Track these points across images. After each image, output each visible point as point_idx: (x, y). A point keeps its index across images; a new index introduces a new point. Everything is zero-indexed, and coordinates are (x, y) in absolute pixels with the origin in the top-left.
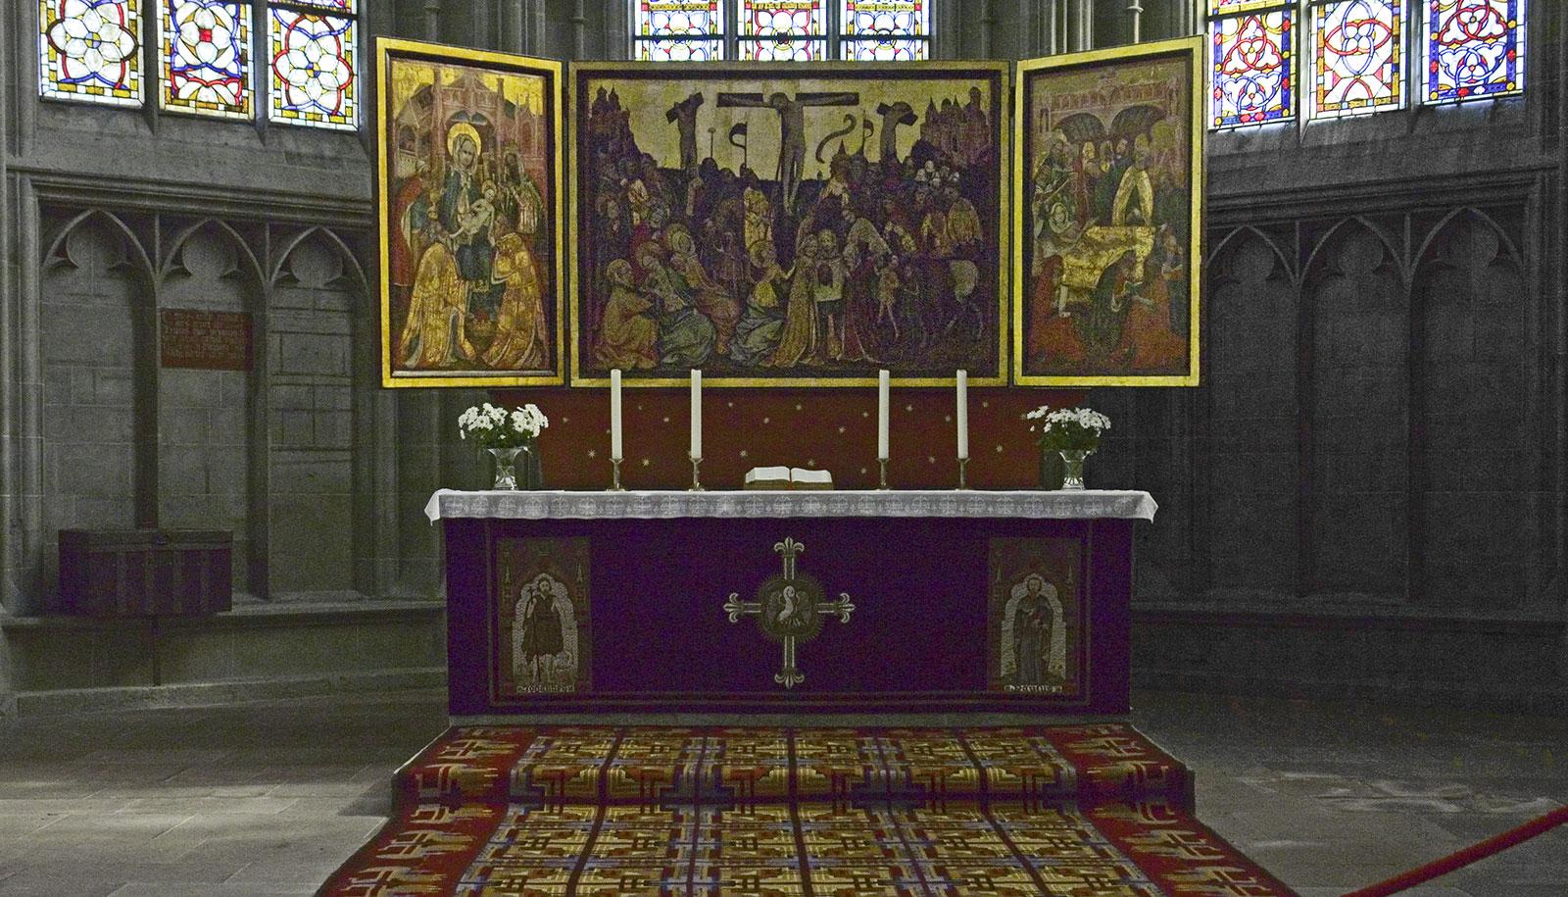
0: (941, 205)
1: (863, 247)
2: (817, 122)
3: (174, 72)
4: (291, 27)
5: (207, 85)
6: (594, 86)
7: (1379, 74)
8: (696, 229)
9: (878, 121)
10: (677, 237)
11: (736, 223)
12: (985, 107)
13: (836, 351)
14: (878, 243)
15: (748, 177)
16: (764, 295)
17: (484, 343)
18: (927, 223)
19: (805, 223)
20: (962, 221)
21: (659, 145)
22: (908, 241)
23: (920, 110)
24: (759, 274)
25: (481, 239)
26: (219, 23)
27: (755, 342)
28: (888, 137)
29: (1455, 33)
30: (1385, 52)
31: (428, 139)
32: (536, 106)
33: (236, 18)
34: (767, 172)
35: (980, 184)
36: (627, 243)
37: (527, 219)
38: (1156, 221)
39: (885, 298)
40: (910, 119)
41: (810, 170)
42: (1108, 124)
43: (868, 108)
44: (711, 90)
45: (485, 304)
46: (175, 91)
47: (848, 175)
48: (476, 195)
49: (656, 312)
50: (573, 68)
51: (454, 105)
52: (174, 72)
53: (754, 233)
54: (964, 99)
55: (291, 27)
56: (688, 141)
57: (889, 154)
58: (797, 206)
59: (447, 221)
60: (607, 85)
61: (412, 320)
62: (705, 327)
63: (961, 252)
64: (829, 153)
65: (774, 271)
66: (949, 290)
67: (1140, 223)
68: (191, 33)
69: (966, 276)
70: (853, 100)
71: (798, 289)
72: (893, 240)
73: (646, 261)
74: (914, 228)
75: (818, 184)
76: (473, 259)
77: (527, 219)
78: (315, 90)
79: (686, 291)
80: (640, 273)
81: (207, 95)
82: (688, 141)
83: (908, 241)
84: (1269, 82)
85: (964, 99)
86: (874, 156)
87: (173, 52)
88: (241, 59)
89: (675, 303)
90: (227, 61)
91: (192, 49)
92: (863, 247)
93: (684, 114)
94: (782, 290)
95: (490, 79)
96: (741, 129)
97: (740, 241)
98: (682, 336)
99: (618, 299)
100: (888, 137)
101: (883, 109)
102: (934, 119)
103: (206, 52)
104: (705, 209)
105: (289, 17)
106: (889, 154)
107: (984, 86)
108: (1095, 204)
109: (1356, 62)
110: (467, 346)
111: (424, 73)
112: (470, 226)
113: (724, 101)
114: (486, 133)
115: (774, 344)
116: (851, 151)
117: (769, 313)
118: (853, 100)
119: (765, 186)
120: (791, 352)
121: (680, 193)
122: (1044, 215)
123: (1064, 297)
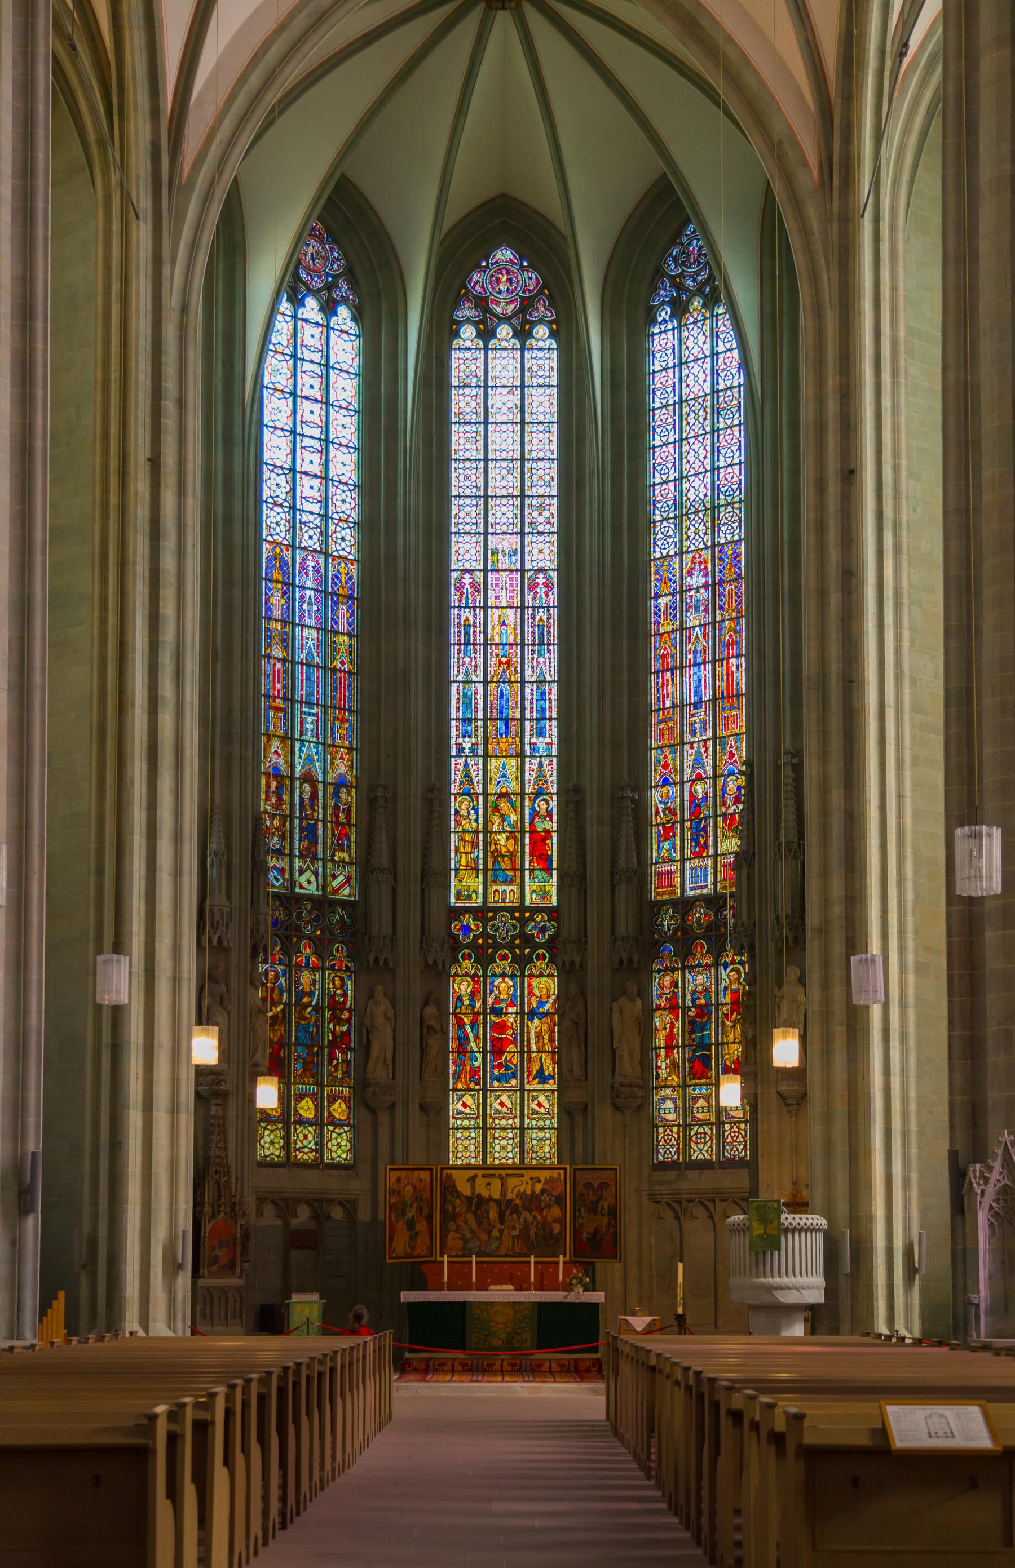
0: (549, 1207)
1: (526, 1220)
2: (512, 1182)
3: (296, 1150)
4: (333, 1131)
5: (306, 1153)
6: (445, 1172)
7: (707, 1151)
8: (476, 1215)
9: (530, 1182)
10: (470, 1216)
11: (487, 1212)
12: (562, 1178)
13: (517, 1249)
14: (530, 1218)
15: (491, 1199)
16: (495, 1233)
17: (413, 1248)
18: (544, 1213)
19: (508, 1212)
20: (555, 1212)
21: (465, 1189)
22: (539, 1217)
23: (543, 1180)
24: (494, 1227)
25: (413, 1218)
26: (310, 1132)
27: (493, 1247)
28: (533, 1186)
29: (729, 1139)
30: (709, 1144)
31: (399, 1192)
32: (428, 1179)
33: (315, 1130)
34: (497, 1196)
35: (560, 1200)
36: (454, 1217)
37: (426, 1212)
38: (609, 1215)
39: (532, 1234)
40: (539, 1181)
41: (510, 1196)
42: (596, 1186)
43: (526, 1178)
44: (480, 1173)
45: (414, 1236)
46: (296, 1156)
47: (521, 1199)
48: (411, 1206)
49: (463, 1238)
50: (439, 1167)
51: (406, 1182)
52: (296, 1150)
53: (493, 1215)
54: (556, 1176)
55: (333, 1131)
56: (473, 1188)
57: (533, 1192)
58: (506, 1207)
59: (404, 1214)
60: (449, 1171)
61: (394, 1243)
62: (478, 1243)
63: (555, 1221)
64: (516, 1190)
65: (499, 1226)
66: (551, 1233)
67: (603, 1215)
68: (301, 1136)
69: (556, 1228)
70: (522, 1176)
71: (506, 1232)
72: (535, 1218)
73: (461, 1223)
74: (541, 1213)
75: (512, 1201)
76: (411, 1224)
77: (426, 1212)
78: (339, 1152)
79: (472, 1232)
80: (458, 1227)
81: (306, 1157)
82: (473, 1188)
83: (539, 1217)
84: (673, 1150)
85: (556, 1176)
86: (529, 1192)
87: (296, 1143)
88: (316, 1144)
89: (468, 1235)
90: (312, 1145)
91: (301, 1142)
92: (526, 1220)
93: (472, 1180)
94: (501, 1232)
95: (416, 1173)
96: (489, 1184)
97: (488, 1217)
98: (471, 1245)
99: (452, 1235)
100: (533, 1186)
101: (531, 1179)
102: (547, 1181)
103: (305, 1142)
104: (479, 1206)
105: (331, 1128)
106: (533, 1192)
107: (562, 1172)
108: (593, 1209)
109: (701, 1146)
110: (409, 1250)
111: (399, 1173)
112: (410, 1215)
113: (484, 1176)
114: (414, 1188)
115: (498, 1248)
116: (522, 1191)
117: (497, 1238)
118: (522, 1176)
119: (496, 1201)
120: (503, 1250)
121: (471, 1203)
122: (579, 1210)
123: (584, 1235)
